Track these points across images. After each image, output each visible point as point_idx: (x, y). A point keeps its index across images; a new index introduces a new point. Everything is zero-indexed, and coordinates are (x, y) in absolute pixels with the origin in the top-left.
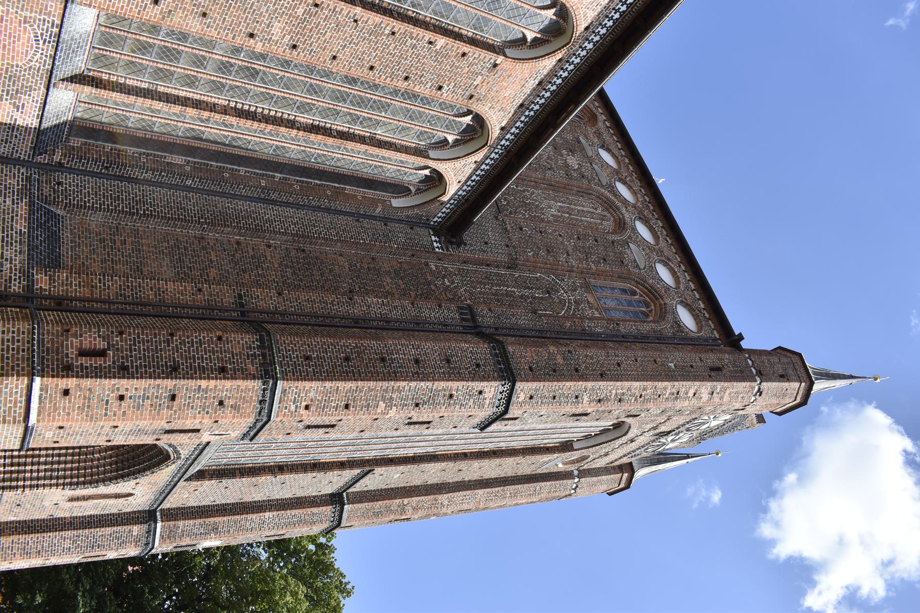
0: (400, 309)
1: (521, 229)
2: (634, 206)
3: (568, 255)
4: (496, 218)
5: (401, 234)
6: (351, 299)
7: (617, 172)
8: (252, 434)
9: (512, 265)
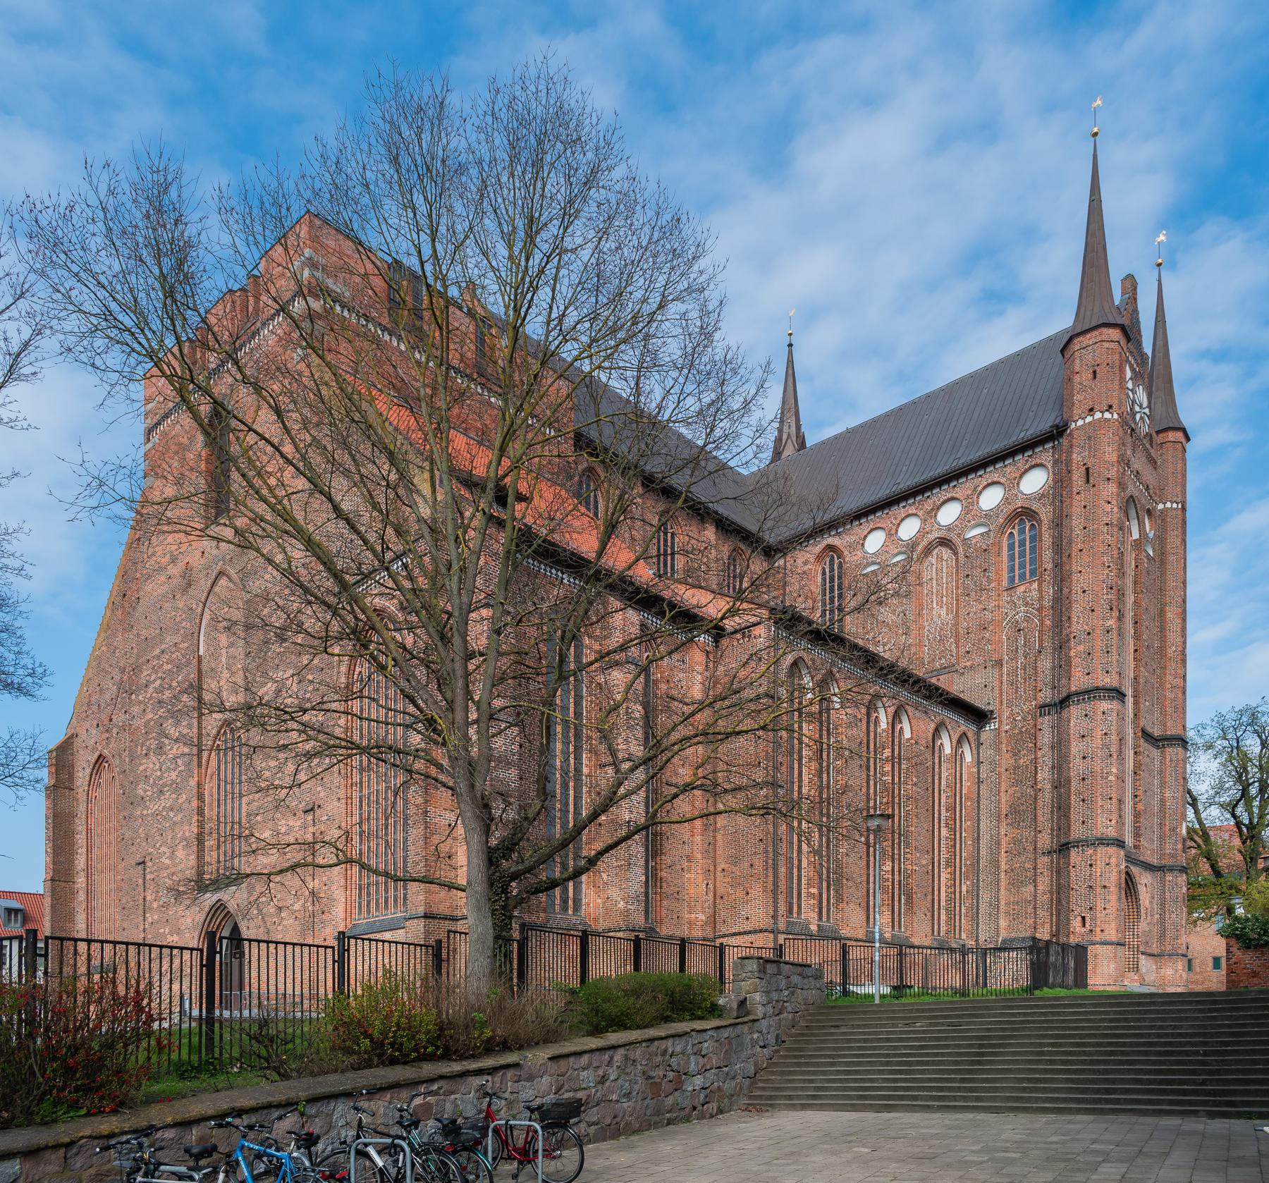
0: (1046, 759)
5: (987, 752)
7: (889, 535)
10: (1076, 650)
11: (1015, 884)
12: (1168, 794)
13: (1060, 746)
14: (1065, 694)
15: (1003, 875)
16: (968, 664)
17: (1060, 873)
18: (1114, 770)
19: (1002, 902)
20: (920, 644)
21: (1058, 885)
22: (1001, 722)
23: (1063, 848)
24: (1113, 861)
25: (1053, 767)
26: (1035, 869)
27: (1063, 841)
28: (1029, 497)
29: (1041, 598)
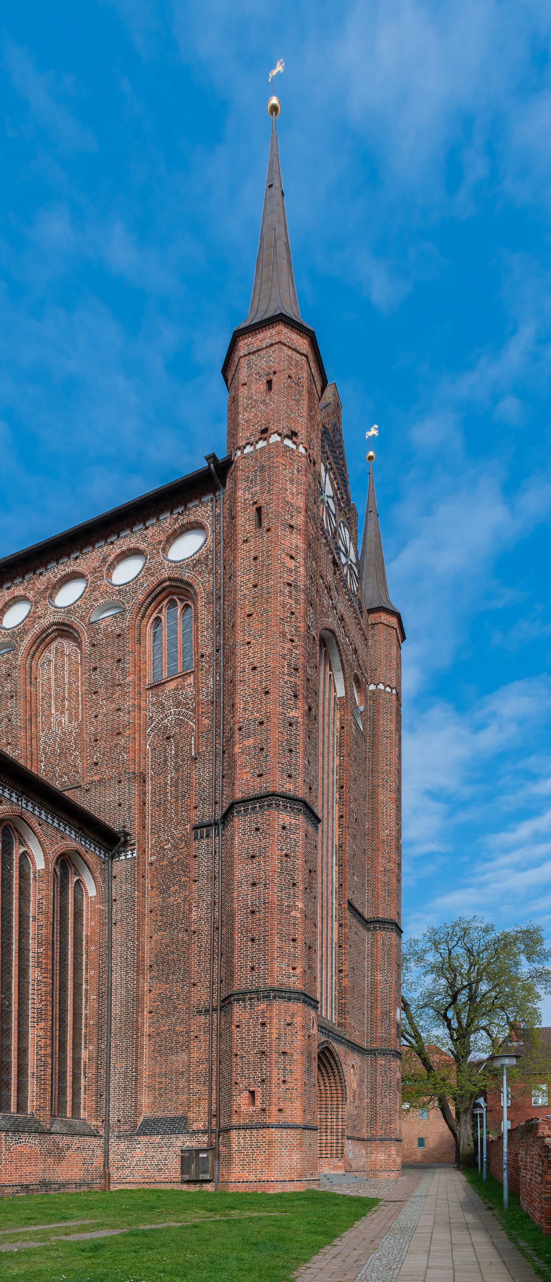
1: (96, 764)
3: (119, 710)
4: (87, 790)
6: (195, 932)
11: (163, 1050)
12: (379, 977)
13: (223, 876)
14: (226, 806)
15: (146, 1041)
16: (96, 778)
17: (222, 1034)
18: (300, 905)
19: (145, 1074)
21: (219, 1051)
23: (226, 1003)
24: (298, 1020)
27: (224, 995)
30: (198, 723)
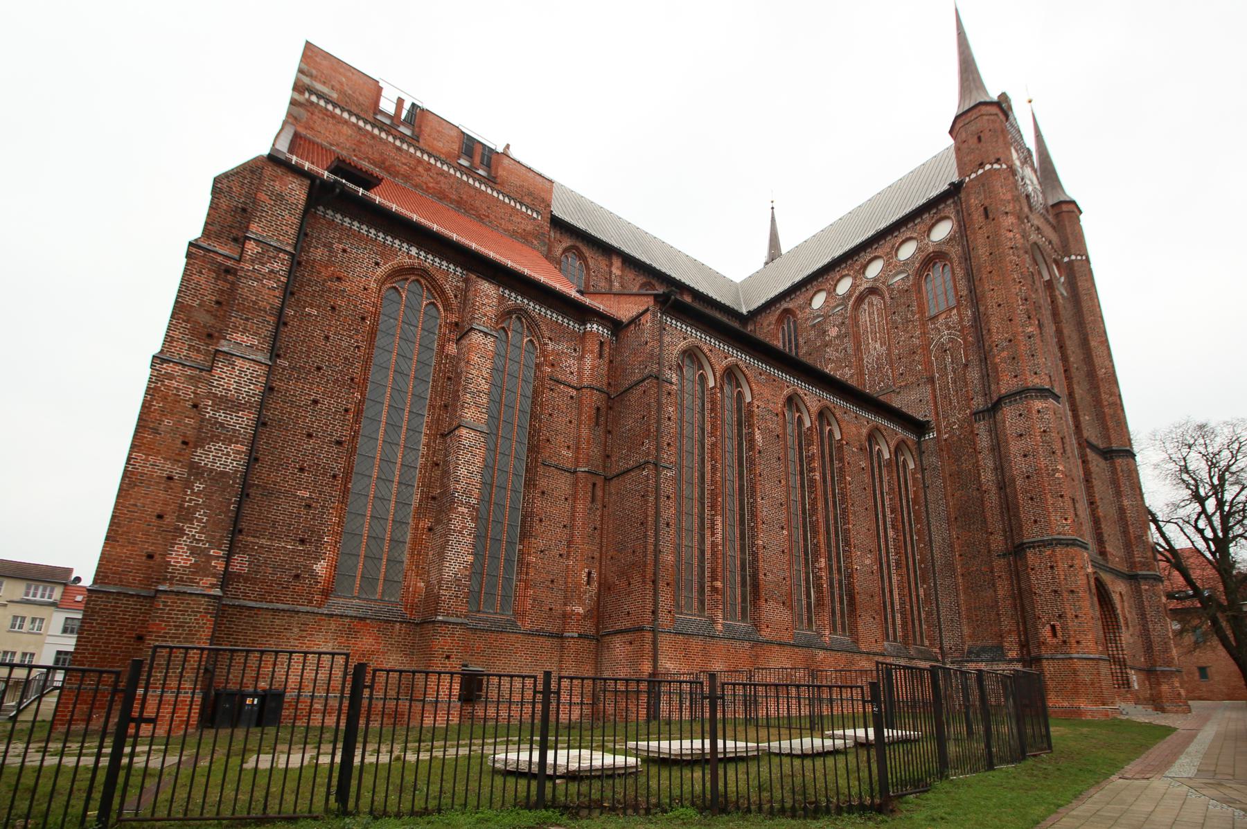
0: (987, 462)
2: (855, 278)
7: (829, 293)
8: (1084, 546)
9: (931, 380)
10: (1000, 357)
13: (998, 448)
20: (861, 374)
22: (939, 432)
25: (996, 469)
26: (992, 572)
28: (940, 243)
29: (962, 319)
30: (965, 340)
